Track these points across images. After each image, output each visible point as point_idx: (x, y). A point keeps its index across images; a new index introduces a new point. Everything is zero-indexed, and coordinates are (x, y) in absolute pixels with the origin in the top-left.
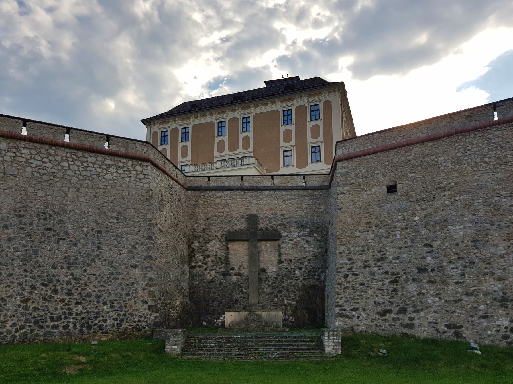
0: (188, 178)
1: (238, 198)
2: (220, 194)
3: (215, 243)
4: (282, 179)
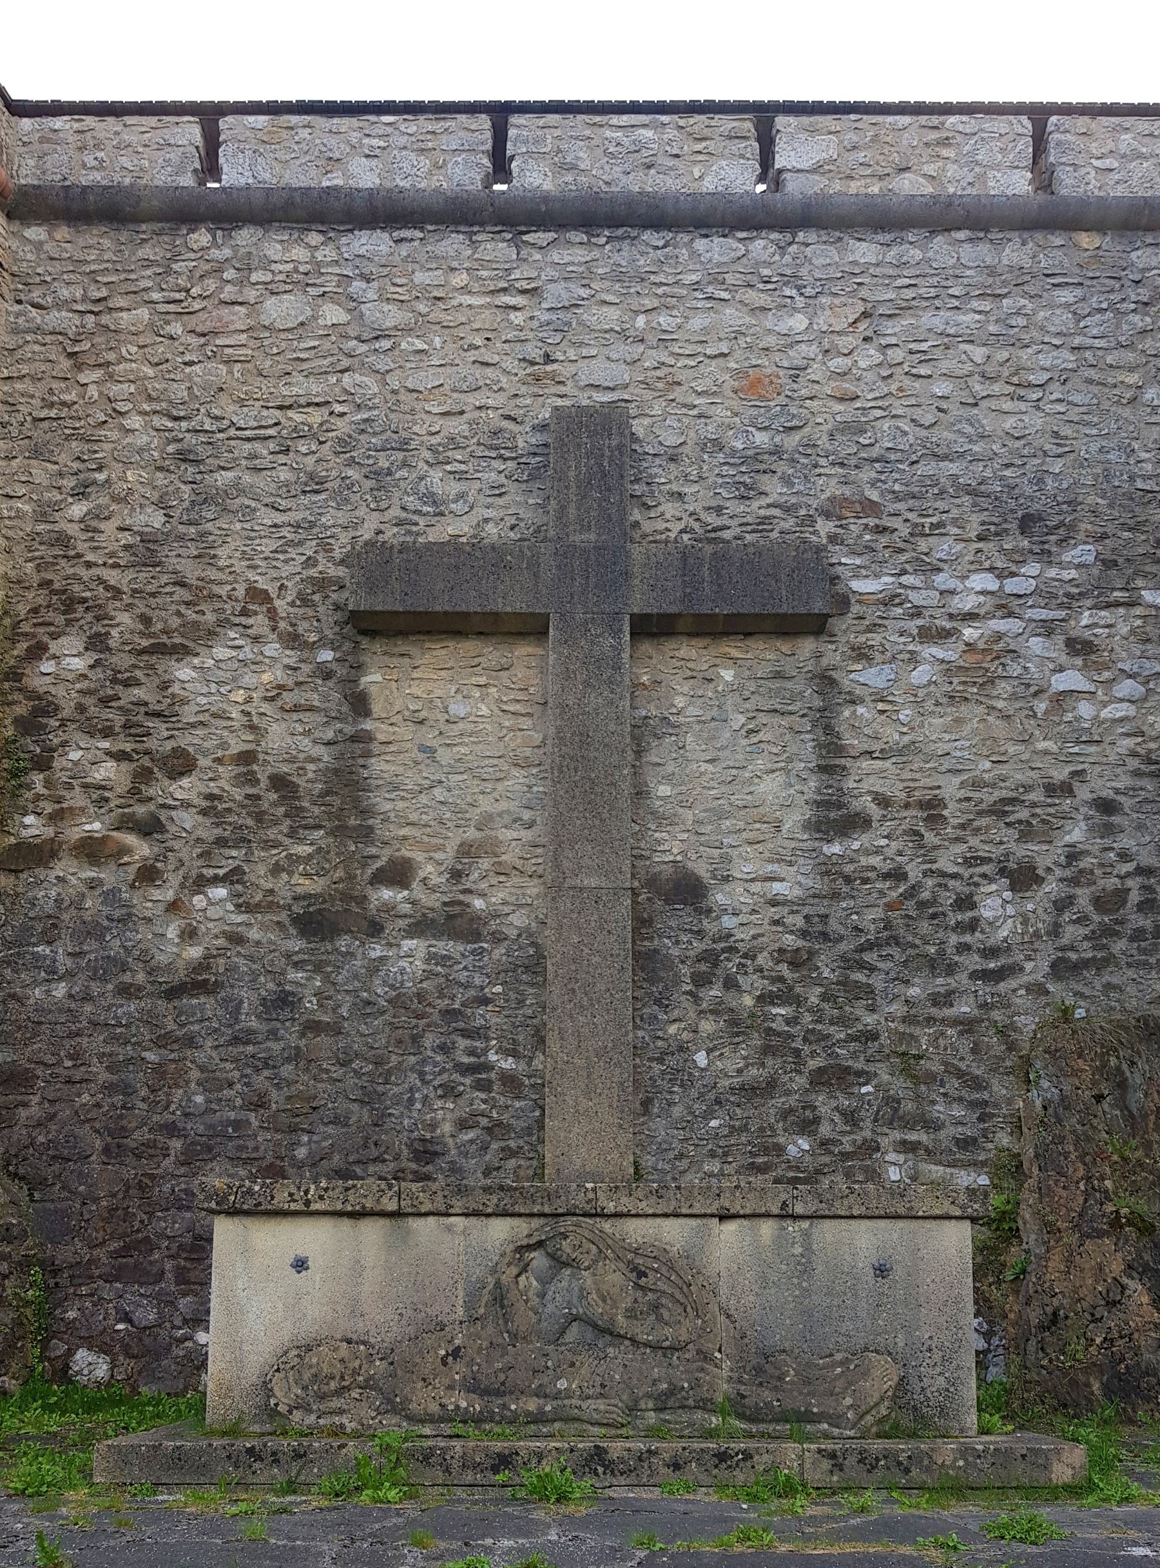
0: (26, 123)
1: (465, 290)
2: (299, 253)
3: (248, 653)
4: (851, 137)
